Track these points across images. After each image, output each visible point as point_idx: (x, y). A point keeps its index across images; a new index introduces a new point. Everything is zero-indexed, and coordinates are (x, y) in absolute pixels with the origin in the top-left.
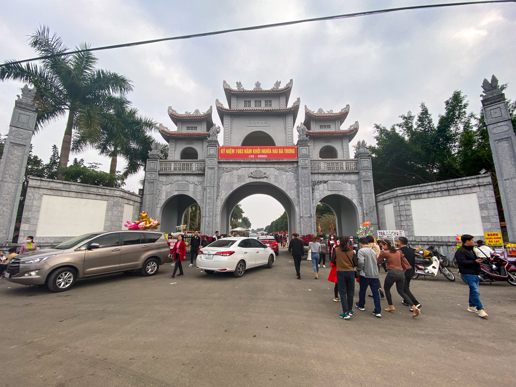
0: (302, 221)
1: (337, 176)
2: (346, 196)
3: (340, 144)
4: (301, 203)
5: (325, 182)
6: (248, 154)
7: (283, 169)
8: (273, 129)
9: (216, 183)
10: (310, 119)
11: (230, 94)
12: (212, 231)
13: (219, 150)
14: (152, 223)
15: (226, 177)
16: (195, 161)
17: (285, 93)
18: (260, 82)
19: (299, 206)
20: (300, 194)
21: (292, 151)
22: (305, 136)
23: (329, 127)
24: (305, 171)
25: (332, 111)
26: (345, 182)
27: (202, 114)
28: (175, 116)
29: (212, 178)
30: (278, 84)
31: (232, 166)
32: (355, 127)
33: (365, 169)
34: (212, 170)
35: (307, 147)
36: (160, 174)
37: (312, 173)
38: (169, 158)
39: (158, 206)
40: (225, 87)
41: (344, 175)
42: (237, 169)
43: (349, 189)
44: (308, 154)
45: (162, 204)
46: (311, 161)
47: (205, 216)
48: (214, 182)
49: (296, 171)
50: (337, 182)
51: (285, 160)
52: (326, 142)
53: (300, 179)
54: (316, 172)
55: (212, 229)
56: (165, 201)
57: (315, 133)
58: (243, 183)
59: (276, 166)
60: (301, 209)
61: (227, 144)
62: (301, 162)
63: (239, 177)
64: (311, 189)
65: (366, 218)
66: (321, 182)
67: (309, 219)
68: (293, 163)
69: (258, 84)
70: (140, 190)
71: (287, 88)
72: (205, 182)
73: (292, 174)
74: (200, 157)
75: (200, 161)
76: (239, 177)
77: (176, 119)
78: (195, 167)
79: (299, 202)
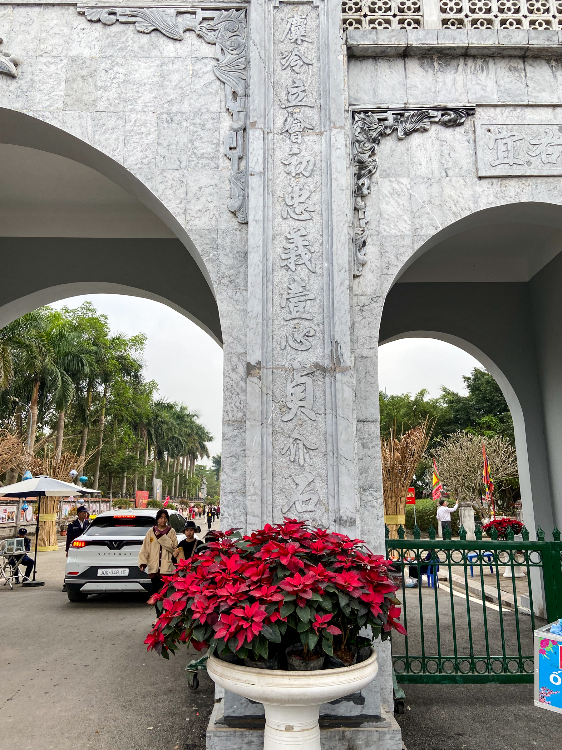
4: (254, 258)
5: (457, 116)
20: (255, 183)
66: (423, 114)
73: (207, 50)
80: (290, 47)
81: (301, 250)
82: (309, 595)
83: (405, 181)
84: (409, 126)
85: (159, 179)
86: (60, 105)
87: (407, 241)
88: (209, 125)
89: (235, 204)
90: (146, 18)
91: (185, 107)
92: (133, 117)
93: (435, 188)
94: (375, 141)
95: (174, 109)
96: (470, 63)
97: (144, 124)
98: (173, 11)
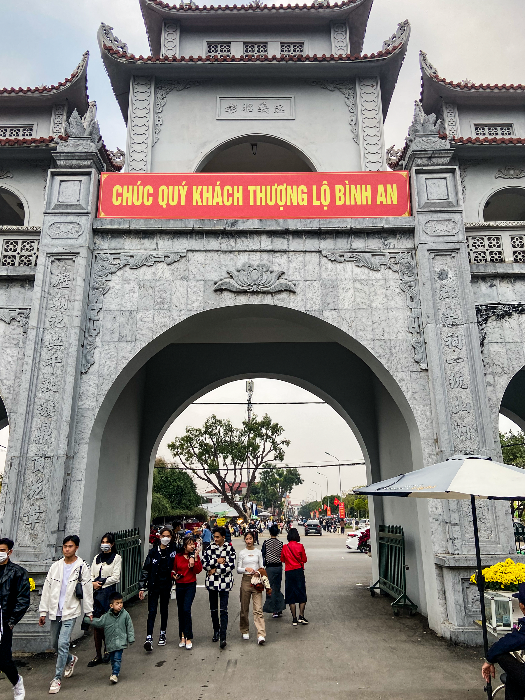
8: (311, 125)
10: (438, 97)
44: (452, 199)
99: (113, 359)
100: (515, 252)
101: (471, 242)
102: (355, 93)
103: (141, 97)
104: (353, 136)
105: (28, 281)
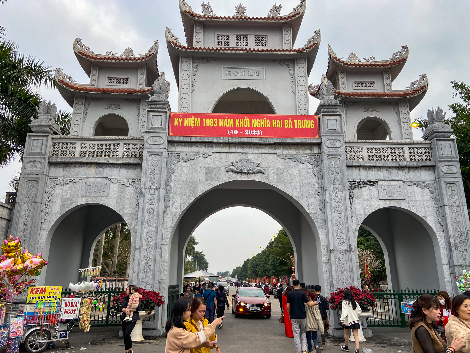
0: (333, 259)
1: (394, 171)
2: (413, 210)
3: (395, 114)
4: (330, 223)
5: (373, 183)
6: (226, 128)
7: (291, 158)
8: (272, 85)
9: (163, 181)
10: (336, 69)
11: (191, 22)
12: (153, 279)
13: (171, 118)
14: (27, 263)
15: (183, 171)
16: (124, 140)
17: (292, 23)
18: (244, 4)
19: (326, 228)
20: (328, 204)
21: (310, 125)
22: (332, 98)
23: (372, 84)
24: (334, 161)
25: (373, 58)
26: (409, 183)
27: (137, 56)
28: (89, 56)
29: (157, 172)
30: (277, 9)
31: (195, 149)
32: (422, 84)
33: (447, 160)
34: (157, 157)
35: (338, 118)
36: (51, 164)
37: (348, 167)
38: (73, 134)
39: (44, 226)
40: (184, 9)
41: (407, 170)
42: (205, 156)
43: (418, 198)
44: (339, 130)
45: (52, 223)
46: (346, 143)
47: (140, 248)
48: (160, 180)
49: (318, 161)
50: (395, 183)
51: (297, 140)
52: (368, 111)
53: (326, 176)
54: (355, 163)
55: (154, 275)
56: (59, 216)
57: (348, 94)
58: (216, 183)
59: (279, 151)
60: (331, 235)
61: (185, 110)
62: (327, 145)
63: (209, 171)
64: (348, 197)
65: (455, 254)
66: (365, 183)
67: (347, 255)
68: (310, 145)
69: (240, 9)
70: (9, 194)
71: (294, 16)
72: (143, 179)
73: (310, 166)
74: (132, 133)
75: (132, 140)
76: (209, 171)
77: (89, 63)
78: (121, 151)
79: (325, 221)
80: (333, 169)
81: (340, 221)
82: (364, 299)
83: (361, 200)
84: (362, 186)
85: (302, 200)
86: (276, 181)
87: (363, 216)
88: (313, 186)
89: (321, 207)
90: (295, 158)
91: (306, 181)
92: (294, 184)
93: (369, 202)
94: (353, 189)
95: (304, 182)
96: (376, 169)
97: (297, 186)
98: (301, 156)
99: (179, 205)
100: (369, 155)
101: (348, 149)
102: (294, 67)
103: (186, 68)
104: (292, 90)
105: (138, 165)
